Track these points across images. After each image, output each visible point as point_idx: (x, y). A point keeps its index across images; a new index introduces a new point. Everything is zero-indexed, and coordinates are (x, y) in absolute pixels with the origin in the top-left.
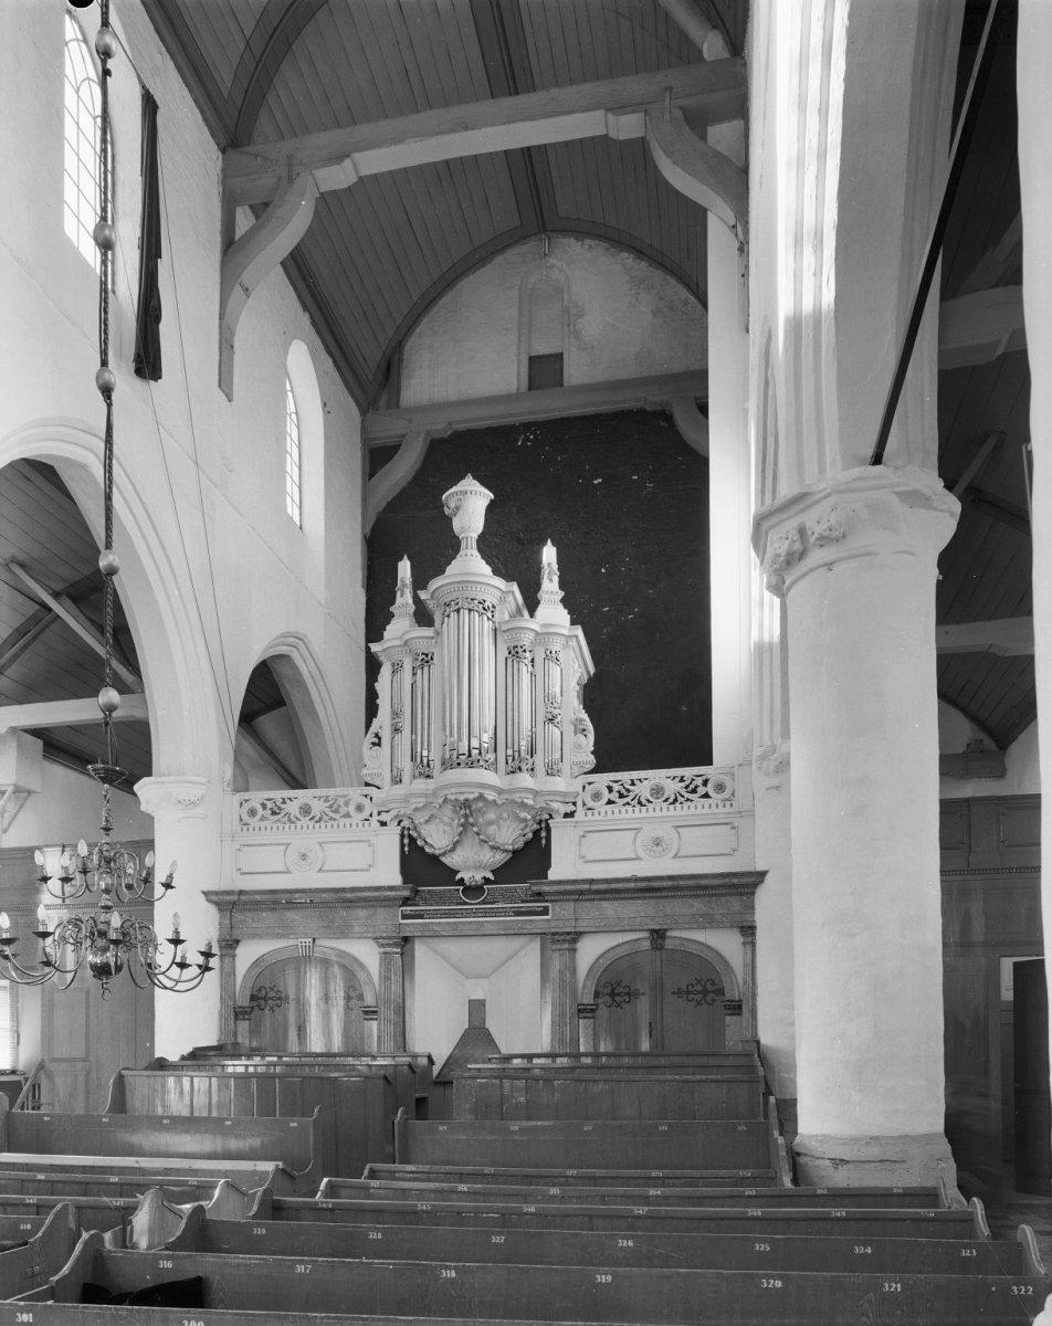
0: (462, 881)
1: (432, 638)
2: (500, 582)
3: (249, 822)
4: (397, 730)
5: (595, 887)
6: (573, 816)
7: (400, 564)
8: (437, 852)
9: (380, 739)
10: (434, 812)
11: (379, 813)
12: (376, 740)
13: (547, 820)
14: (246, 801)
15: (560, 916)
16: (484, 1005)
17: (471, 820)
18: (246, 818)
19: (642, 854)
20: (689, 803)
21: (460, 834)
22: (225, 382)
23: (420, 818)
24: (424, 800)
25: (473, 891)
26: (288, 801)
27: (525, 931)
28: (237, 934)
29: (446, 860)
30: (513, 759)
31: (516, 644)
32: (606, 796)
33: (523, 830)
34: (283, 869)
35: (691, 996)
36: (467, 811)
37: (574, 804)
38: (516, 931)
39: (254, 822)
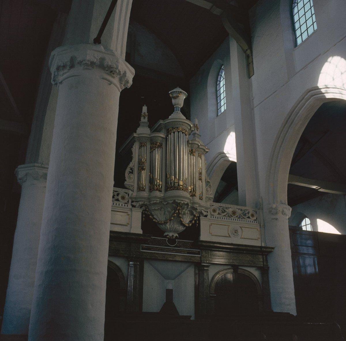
6: (207, 217)
7: (143, 107)
9: (132, 171)
11: (132, 202)
12: (131, 171)
19: (230, 234)
20: (244, 219)
25: (172, 241)
29: (162, 227)
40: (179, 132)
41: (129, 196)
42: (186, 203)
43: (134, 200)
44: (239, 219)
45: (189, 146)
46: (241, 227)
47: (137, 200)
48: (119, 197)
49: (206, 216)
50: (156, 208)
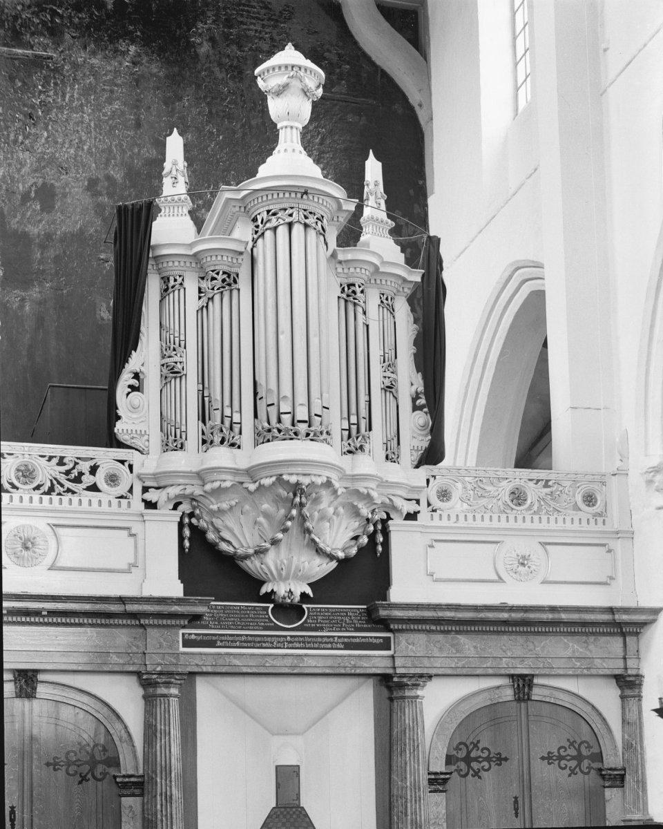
0: (269, 597)
4: (172, 373)
6: (415, 519)
11: (145, 489)
12: (135, 382)
13: (384, 522)
15: (410, 650)
16: (298, 775)
19: (504, 575)
24: (229, 477)
25: (289, 610)
27: (358, 671)
29: (253, 566)
30: (349, 436)
31: (351, 281)
35: (563, 763)
36: (295, 497)
37: (418, 502)
40: (290, 225)
41: (131, 472)
42: (319, 481)
43: (148, 484)
44: (536, 518)
45: (340, 270)
46: (544, 544)
47: (162, 484)
48: (100, 479)
49: (412, 516)
50: (225, 506)
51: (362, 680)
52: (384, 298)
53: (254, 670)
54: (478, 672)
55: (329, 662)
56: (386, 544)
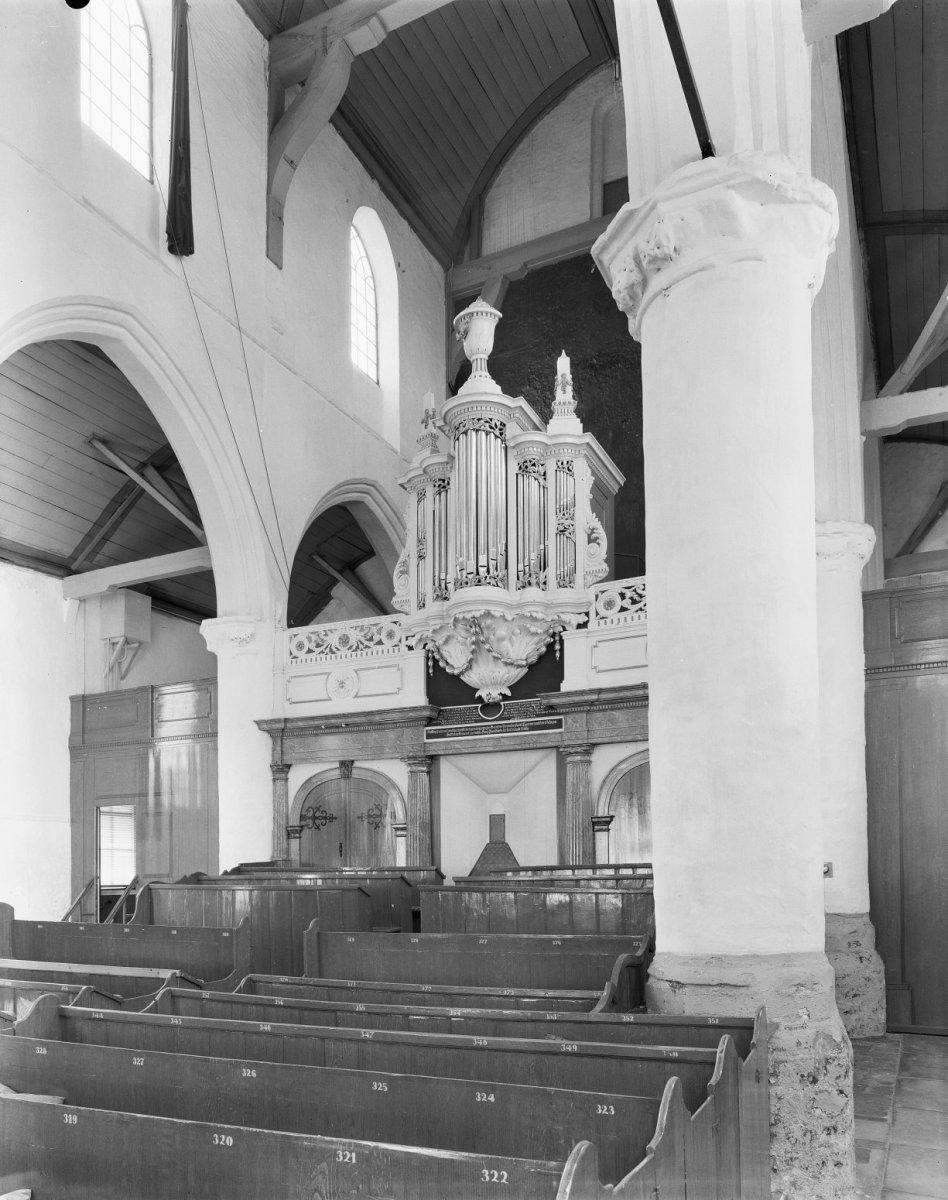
1: (447, 463)
2: (508, 400)
3: (297, 655)
4: (421, 557)
5: (603, 696)
8: (456, 672)
10: (451, 633)
14: (295, 636)
15: (574, 727)
17: (482, 638)
18: (295, 652)
21: (473, 652)
22: (274, 251)
23: (440, 640)
25: (490, 707)
26: (329, 633)
27: (539, 746)
28: (287, 760)
32: (619, 603)
33: (536, 644)
34: (326, 697)
37: (587, 614)
38: (532, 746)
39: (302, 655)
49: (582, 626)
51: (549, 750)
52: (559, 464)
53: (470, 751)
54: (630, 738)
55: (518, 741)
56: (562, 650)
